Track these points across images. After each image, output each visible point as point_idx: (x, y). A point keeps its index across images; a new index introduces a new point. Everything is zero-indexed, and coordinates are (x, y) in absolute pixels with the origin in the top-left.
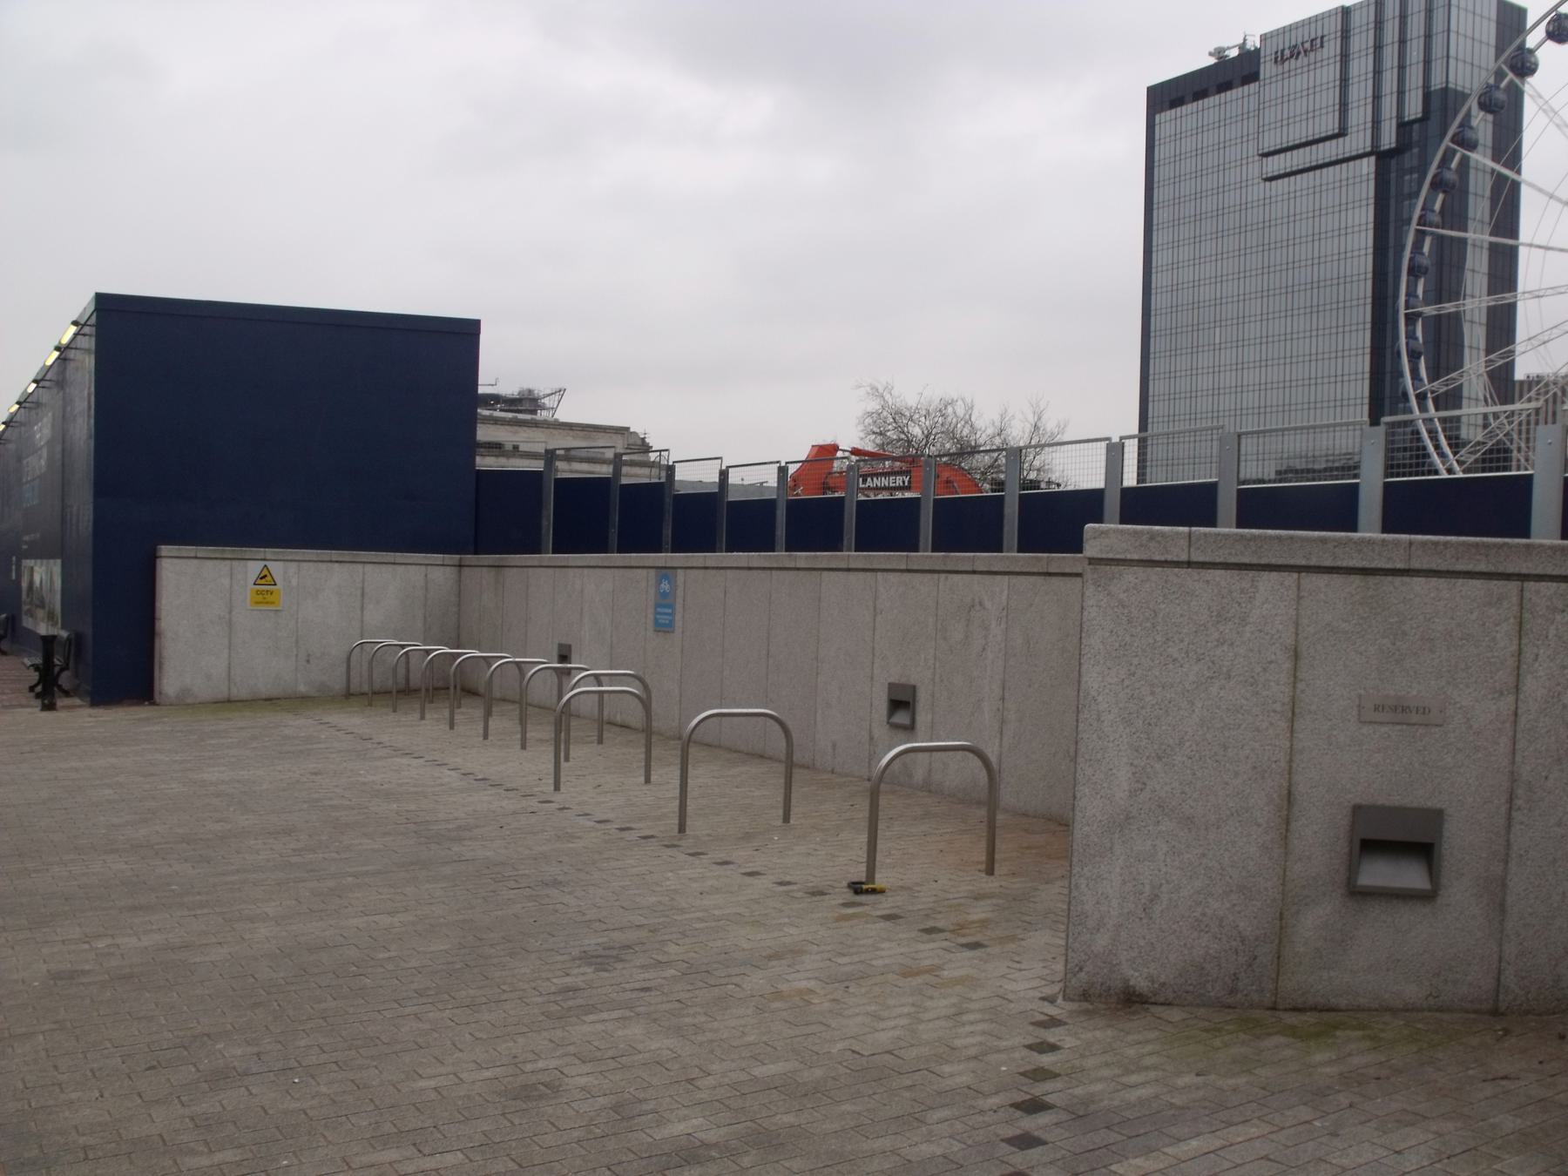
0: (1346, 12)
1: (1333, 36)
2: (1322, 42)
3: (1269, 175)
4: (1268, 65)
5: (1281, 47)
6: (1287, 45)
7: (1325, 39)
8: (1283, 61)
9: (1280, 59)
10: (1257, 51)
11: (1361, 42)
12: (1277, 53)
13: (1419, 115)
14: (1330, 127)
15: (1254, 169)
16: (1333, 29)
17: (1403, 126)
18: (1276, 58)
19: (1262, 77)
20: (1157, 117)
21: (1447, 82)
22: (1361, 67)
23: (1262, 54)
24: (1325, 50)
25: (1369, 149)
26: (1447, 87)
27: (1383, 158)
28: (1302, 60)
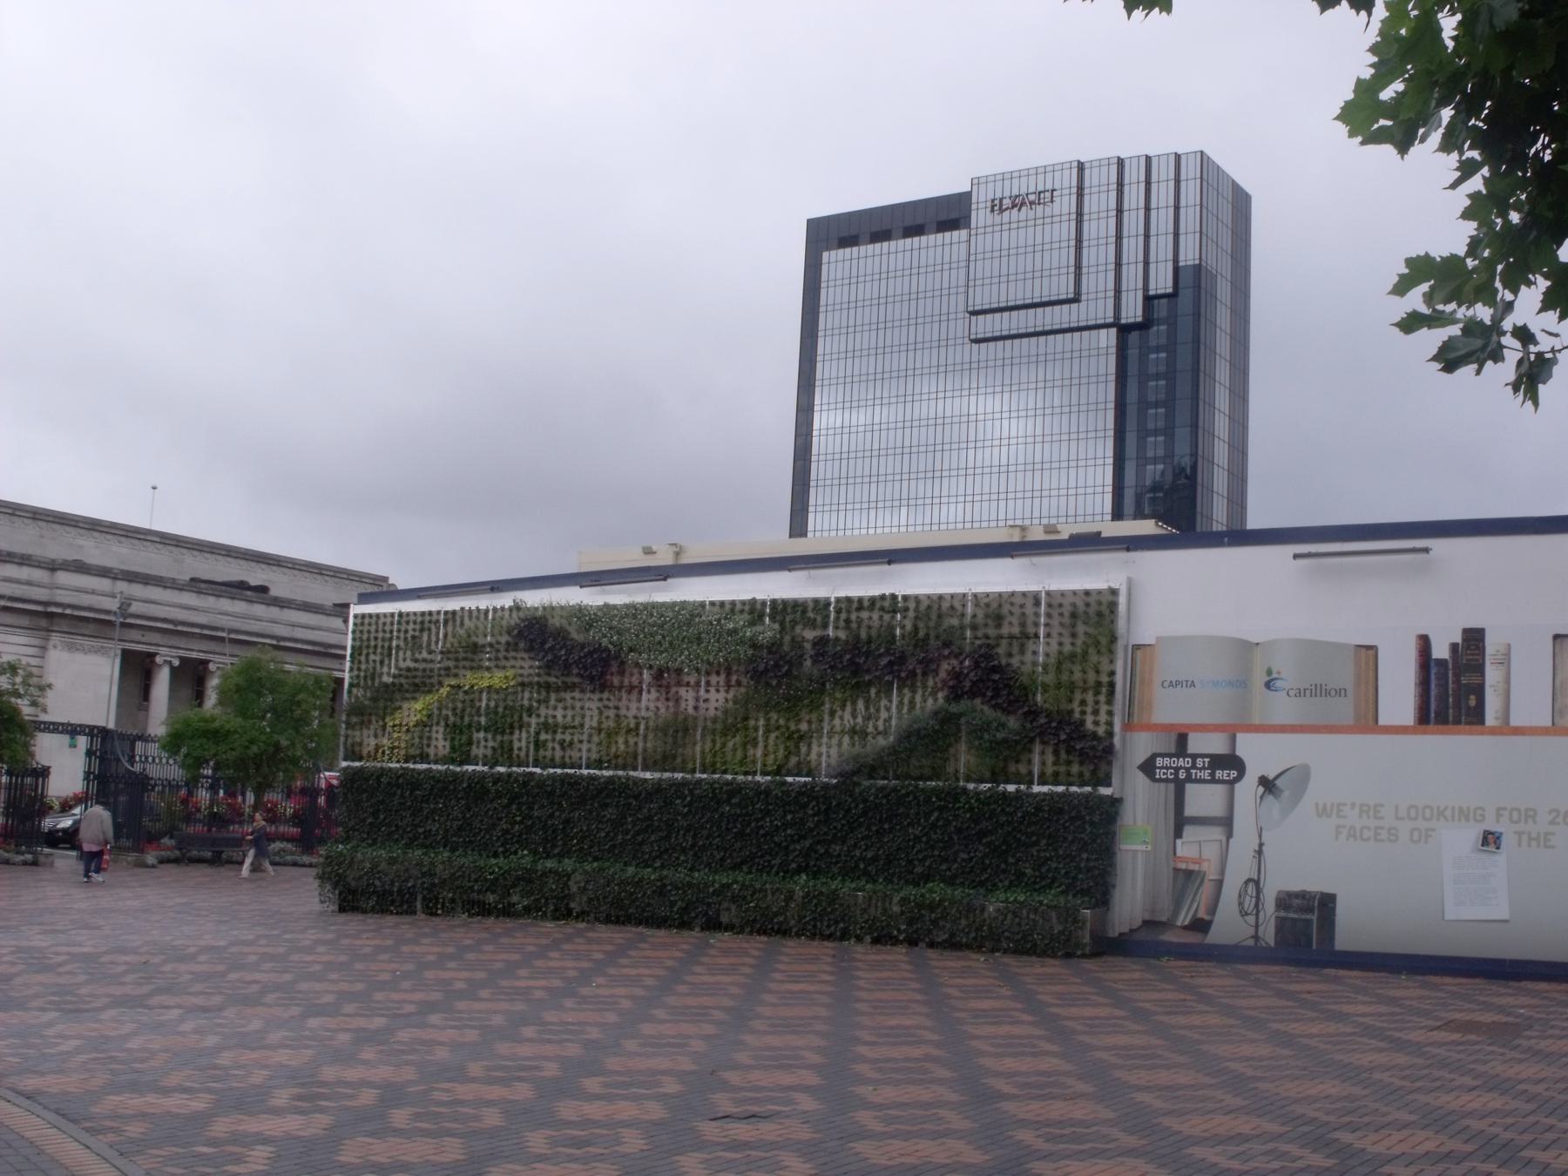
3: (979, 336)
4: (981, 212)
5: (998, 195)
6: (1007, 194)
8: (1001, 211)
9: (997, 206)
10: (968, 195)
11: (1100, 202)
12: (993, 201)
15: (960, 327)
16: (1066, 184)
18: (993, 207)
19: (973, 225)
20: (825, 255)
23: (974, 199)
25: (1111, 320)
26: (1200, 264)
27: (1124, 330)
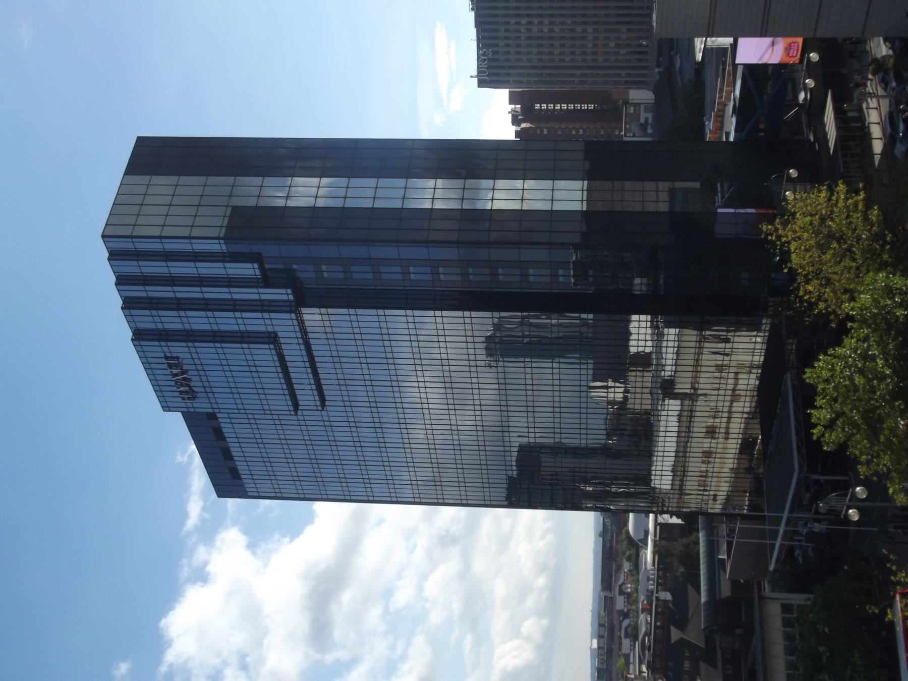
0: (139, 336)
1: (166, 349)
2: (173, 358)
3: (318, 403)
4: (195, 405)
5: (177, 394)
7: (168, 355)
11: (172, 320)
13: (256, 265)
14: (268, 352)
16: (159, 349)
17: (266, 280)
19: (211, 411)
21: (218, 238)
22: (199, 321)
23: (186, 410)
24: (180, 355)
28: (192, 374)
